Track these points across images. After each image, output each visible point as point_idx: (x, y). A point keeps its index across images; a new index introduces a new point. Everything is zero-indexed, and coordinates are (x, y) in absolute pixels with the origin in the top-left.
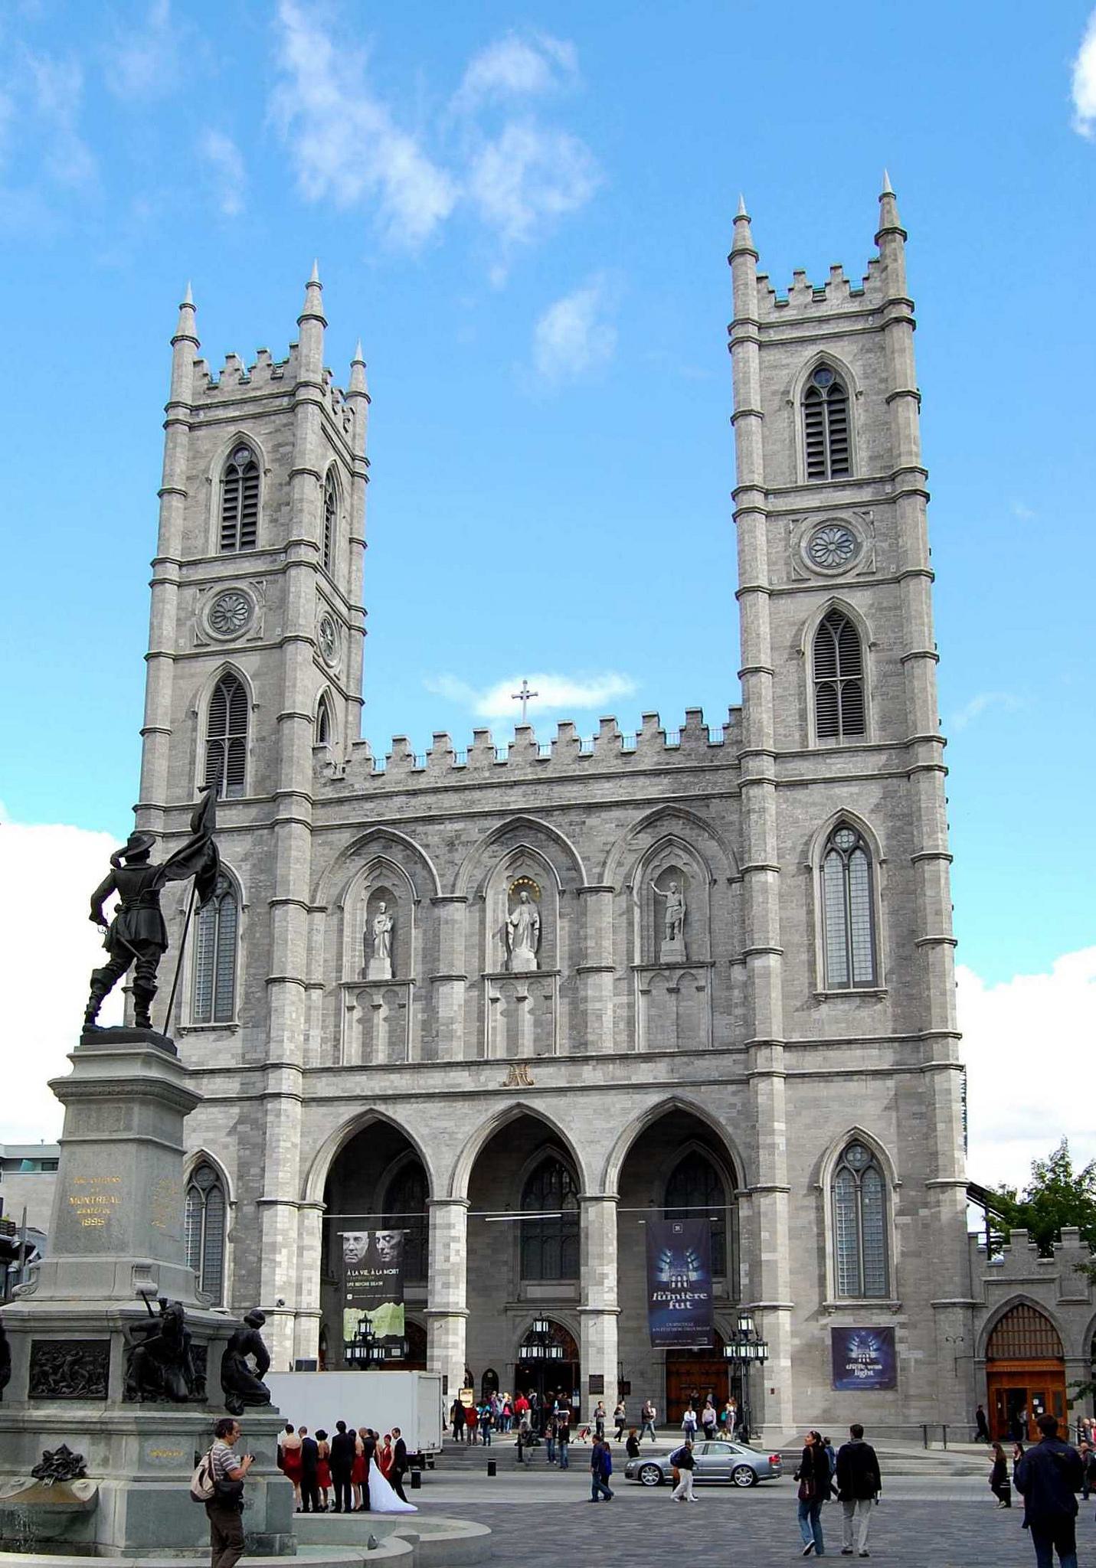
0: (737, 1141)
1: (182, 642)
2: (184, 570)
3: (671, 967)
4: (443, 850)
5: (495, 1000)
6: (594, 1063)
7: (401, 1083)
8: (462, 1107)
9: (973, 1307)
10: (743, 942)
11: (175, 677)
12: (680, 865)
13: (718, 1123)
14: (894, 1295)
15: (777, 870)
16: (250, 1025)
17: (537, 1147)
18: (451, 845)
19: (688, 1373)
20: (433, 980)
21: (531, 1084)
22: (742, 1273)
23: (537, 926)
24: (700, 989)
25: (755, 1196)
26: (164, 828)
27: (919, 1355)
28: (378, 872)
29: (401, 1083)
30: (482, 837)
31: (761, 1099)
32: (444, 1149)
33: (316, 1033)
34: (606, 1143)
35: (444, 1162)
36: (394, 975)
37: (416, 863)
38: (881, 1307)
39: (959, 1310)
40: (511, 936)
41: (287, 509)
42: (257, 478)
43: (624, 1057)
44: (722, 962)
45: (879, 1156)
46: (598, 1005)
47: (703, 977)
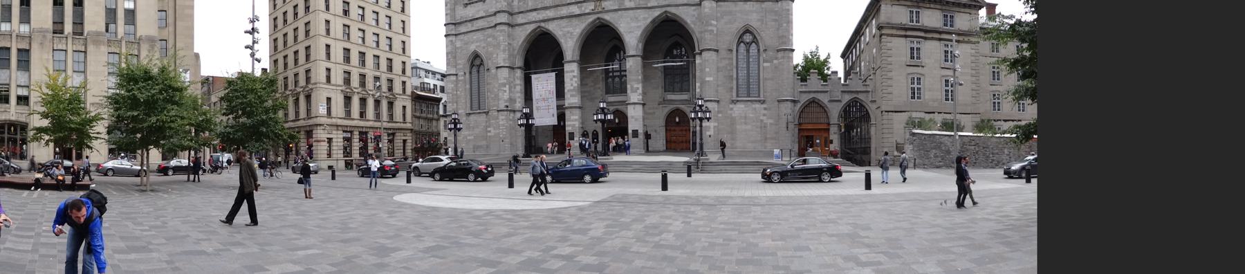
0: (695, 30)
7: (550, 14)
8: (575, 21)
9: (794, 102)
13: (686, 23)
14: (762, 96)
19: (675, 130)
25: (703, 53)
27: (771, 121)
29: (550, 14)
31: (706, 10)
32: (569, 40)
34: (637, 32)
35: (569, 45)
38: (756, 101)
39: (789, 103)
45: (758, 38)
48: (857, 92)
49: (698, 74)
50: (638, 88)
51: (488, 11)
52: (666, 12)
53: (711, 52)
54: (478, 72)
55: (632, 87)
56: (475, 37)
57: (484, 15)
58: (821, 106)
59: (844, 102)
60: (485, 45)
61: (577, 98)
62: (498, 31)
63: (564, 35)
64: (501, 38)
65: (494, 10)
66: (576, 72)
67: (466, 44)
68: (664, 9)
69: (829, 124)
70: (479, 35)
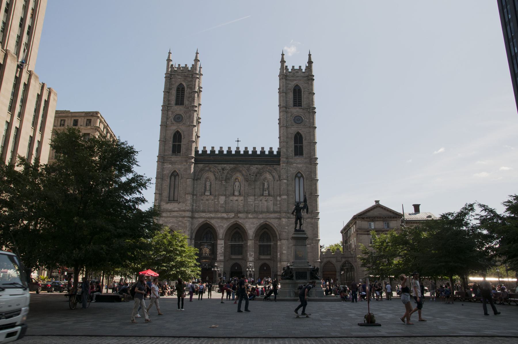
1: (168, 123)
2: (169, 108)
3: (265, 196)
4: (221, 170)
5: (232, 200)
6: (251, 214)
7: (212, 215)
8: (225, 221)
10: (280, 193)
11: (166, 130)
15: (287, 180)
17: (235, 229)
18: (223, 169)
20: (219, 195)
21: (239, 217)
22: (278, 255)
24: (271, 201)
26: (164, 161)
29: (212, 215)
32: (221, 229)
36: (211, 194)
37: (216, 172)
41: (190, 98)
42: (184, 91)
46: (252, 203)
47: (271, 198)
48: (348, 258)
49: (279, 249)
50: (252, 255)
52: (266, 221)
53: (286, 240)
55: (250, 254)
56: (171, 220)
57: (178, 210)
58: (332, 264)
59: (342, 262)
61: (223, 257)
64: (188, 224)
66: (223, 244)
67: (166, 223)
68: (265, 220)
69: (336, 272)
70: (174, 220)
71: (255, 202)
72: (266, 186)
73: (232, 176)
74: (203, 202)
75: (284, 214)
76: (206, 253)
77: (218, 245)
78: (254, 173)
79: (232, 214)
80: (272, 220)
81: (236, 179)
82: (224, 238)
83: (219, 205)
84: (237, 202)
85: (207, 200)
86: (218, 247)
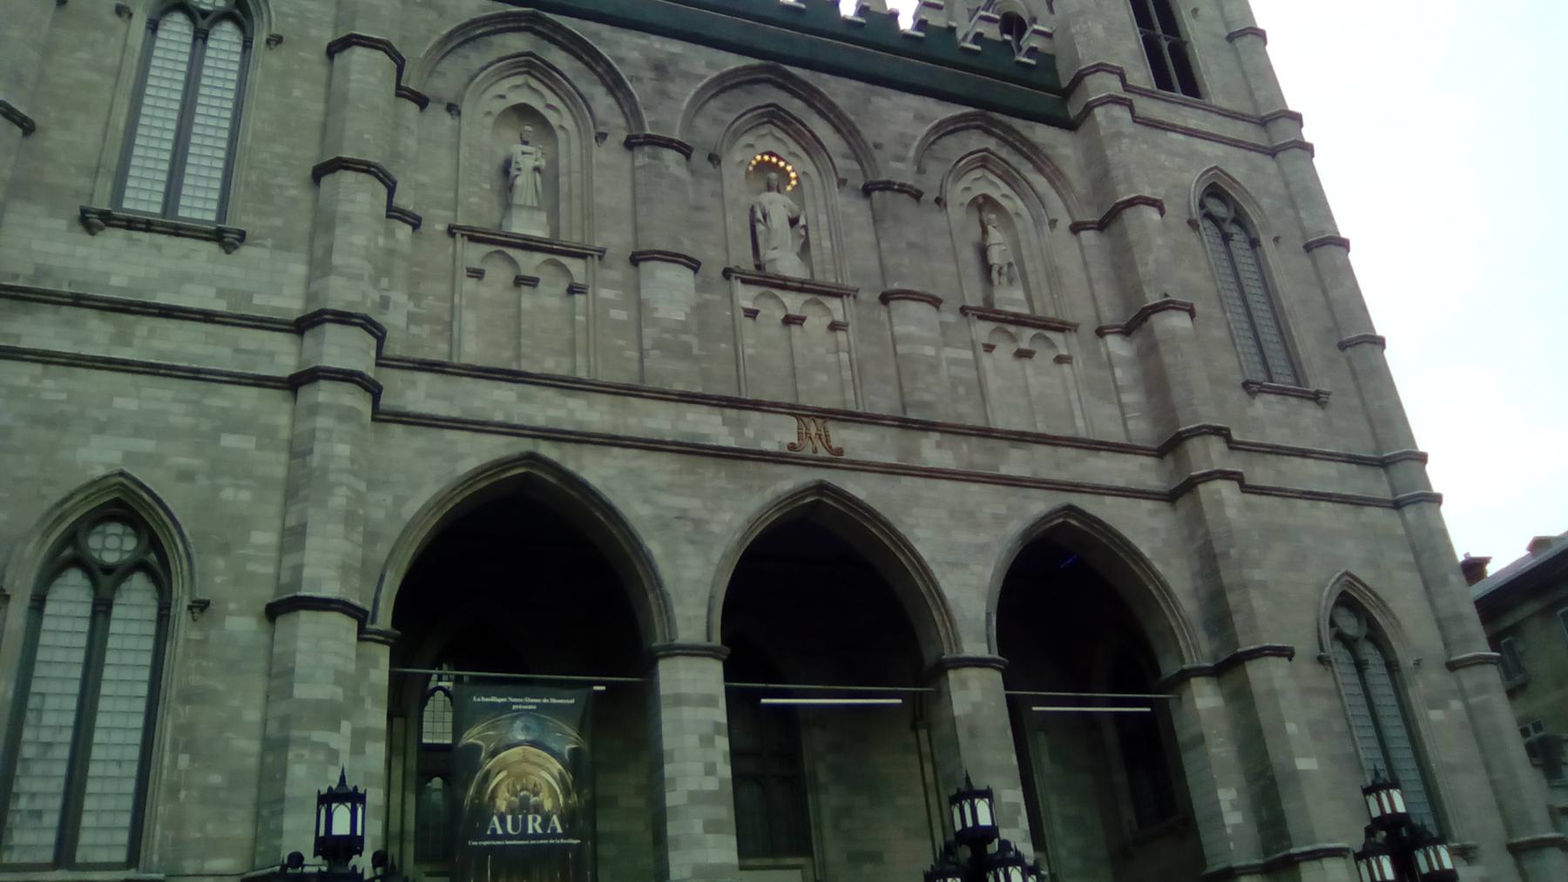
4: (648, 74)
8: (713, 475)
12: (995, 195)
16: (269, 242)
21: (840, 452)
22: (1225, 806)
23: (802, 222)
24: (1060, 360)
28: (519, 80)
30: (715, 74)
32: (686, 548)
33: (399, 297)
40: (760, 228)
43: (985, 433)
44: (1088, 328)
46: (929, 351)
51: (248, 296)
52: (1070, 510)
54: (102, 610)
57: (220, 306)
60: (195, 462)
62: (314, 410)
63: (663, 525)
64: (343, 450)
65: (292, 304)
71: (950, 353)
72: (995, 257)
73: (737, 135)
74: (485, 291)
75: (1216, 445)
76: (524, 808)
77: (667, 715)
78: (907, 146)
79: (771, 417)
80: (1108, 500)
81: (763, 167)
82: (717, 640)
83: (649, 333)
84: (795, 329)
85: (520, 281)
86: (666, 728)
